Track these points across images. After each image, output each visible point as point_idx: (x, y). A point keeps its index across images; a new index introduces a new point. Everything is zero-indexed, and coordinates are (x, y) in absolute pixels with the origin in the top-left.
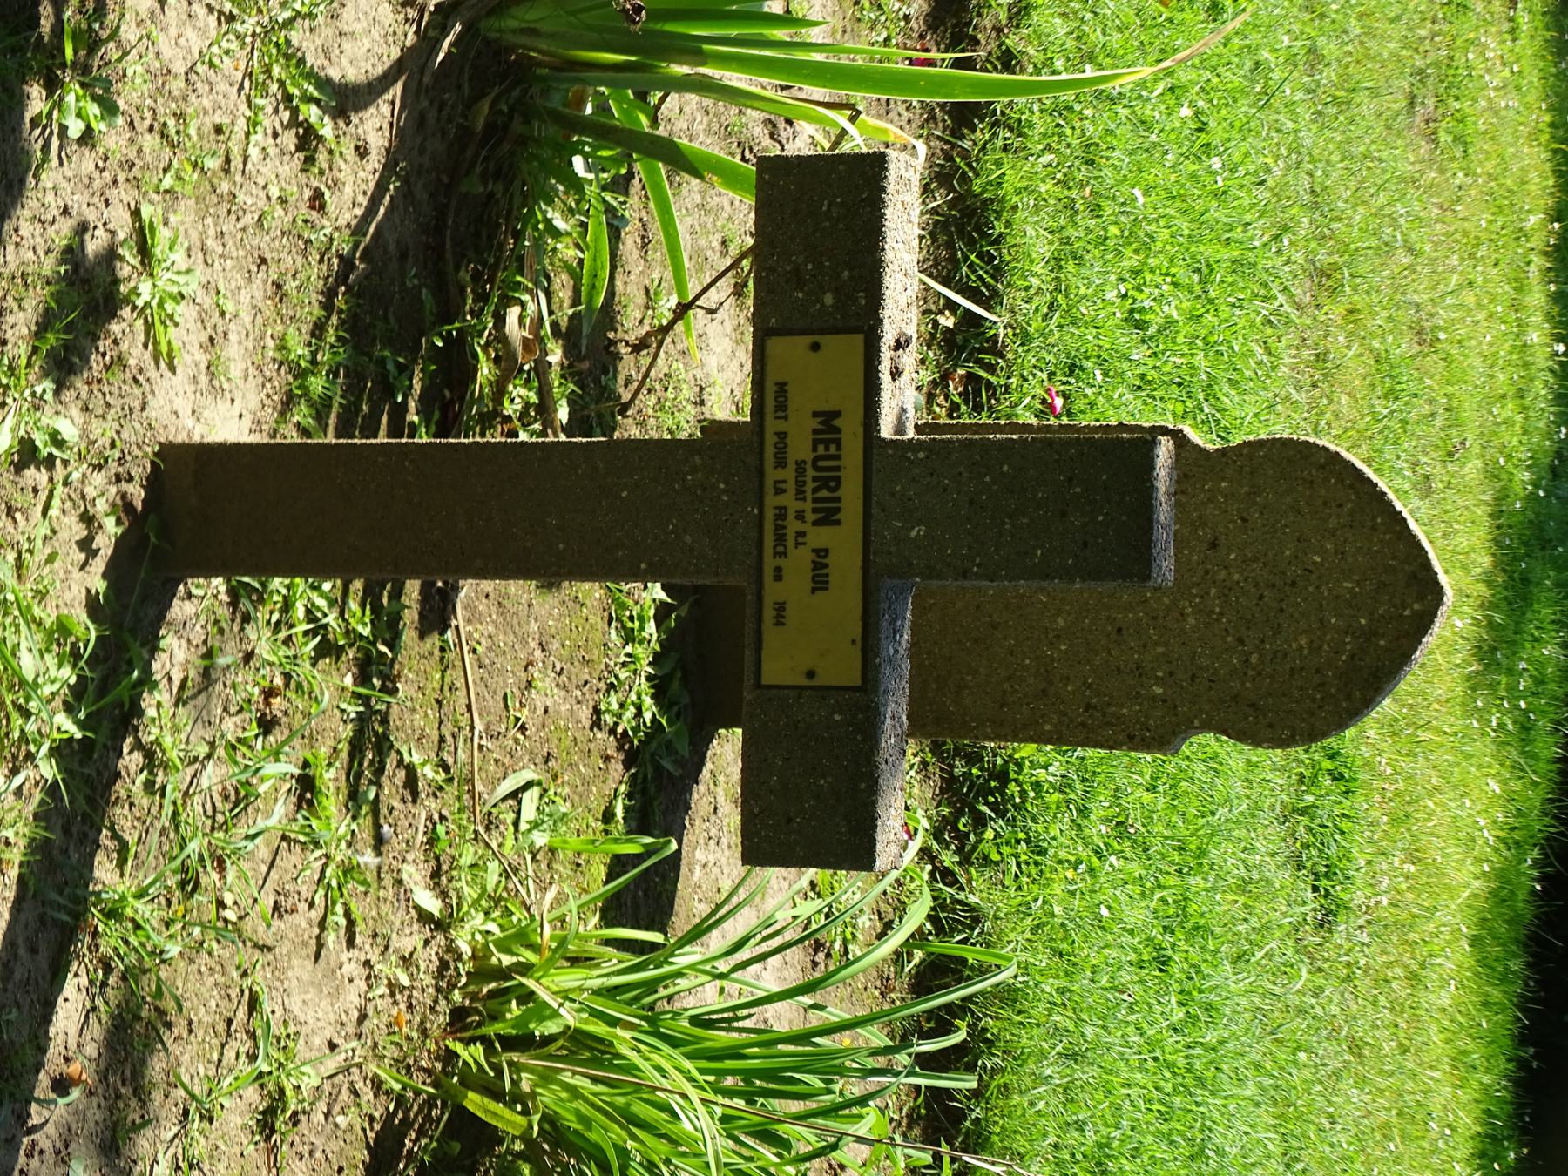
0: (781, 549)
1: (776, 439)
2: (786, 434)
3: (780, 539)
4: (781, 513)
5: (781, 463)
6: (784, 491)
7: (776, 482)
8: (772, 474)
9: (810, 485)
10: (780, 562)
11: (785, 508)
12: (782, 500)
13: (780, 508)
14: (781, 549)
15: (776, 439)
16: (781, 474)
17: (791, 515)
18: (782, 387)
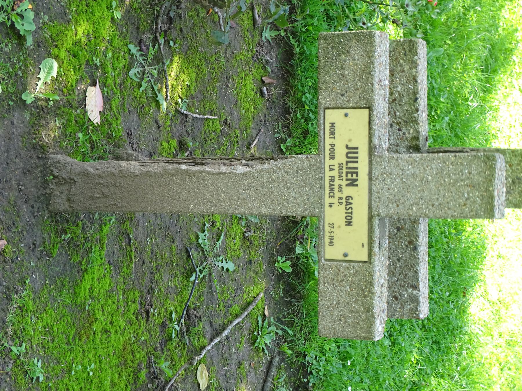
0: (332, 194)
1: (331, 147)
2: (334, 145)
3: (332, 190)
4: (332, 179)
5: (332, 157)
6: (333, 169)
7: (330, 166)
8: (328, 162)
9: (344, 170)
10: (331, 200)
11: (334, 177)
12: (332, 173)
13: (332, 177)
14: (332, 194)
15: (331, 147)
16: (332, 162)
17: (337, 178)
18: (333, 125)
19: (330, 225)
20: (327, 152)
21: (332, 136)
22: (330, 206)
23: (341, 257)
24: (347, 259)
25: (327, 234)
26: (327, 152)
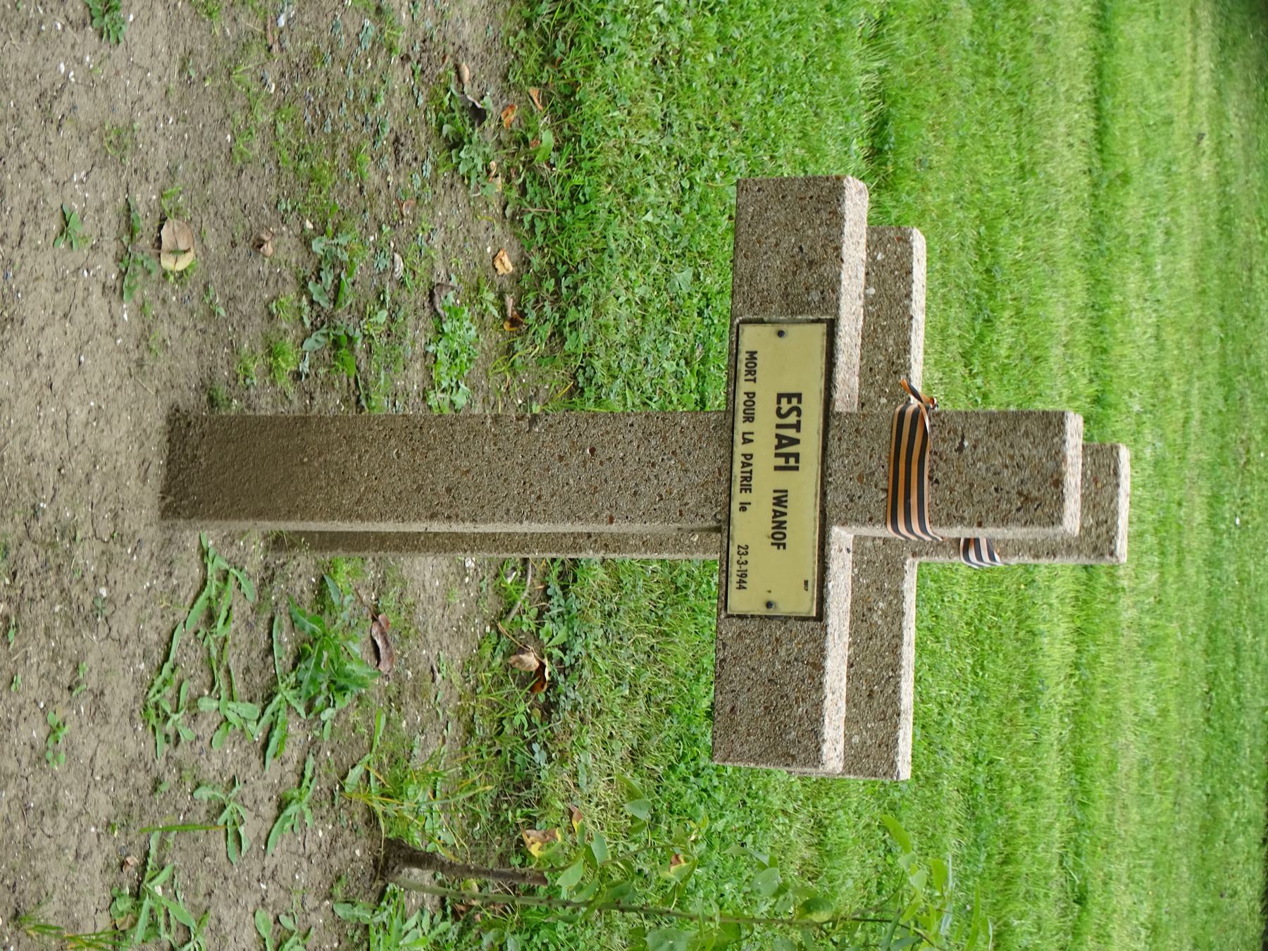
1: (745, 398)
3: (747, 478)
5: (749, 418)
6: (751, 441)
8: (741, 427)
12: (747, 449)
16: (746, 427)
18: (752, 355)
19: (742, 551)
20: (740, 408)
21: (750, 377)
22: (743, 509)
23: (762, 611)
24: (771, 612)
25: (734, 569)
26: (740, 408)
